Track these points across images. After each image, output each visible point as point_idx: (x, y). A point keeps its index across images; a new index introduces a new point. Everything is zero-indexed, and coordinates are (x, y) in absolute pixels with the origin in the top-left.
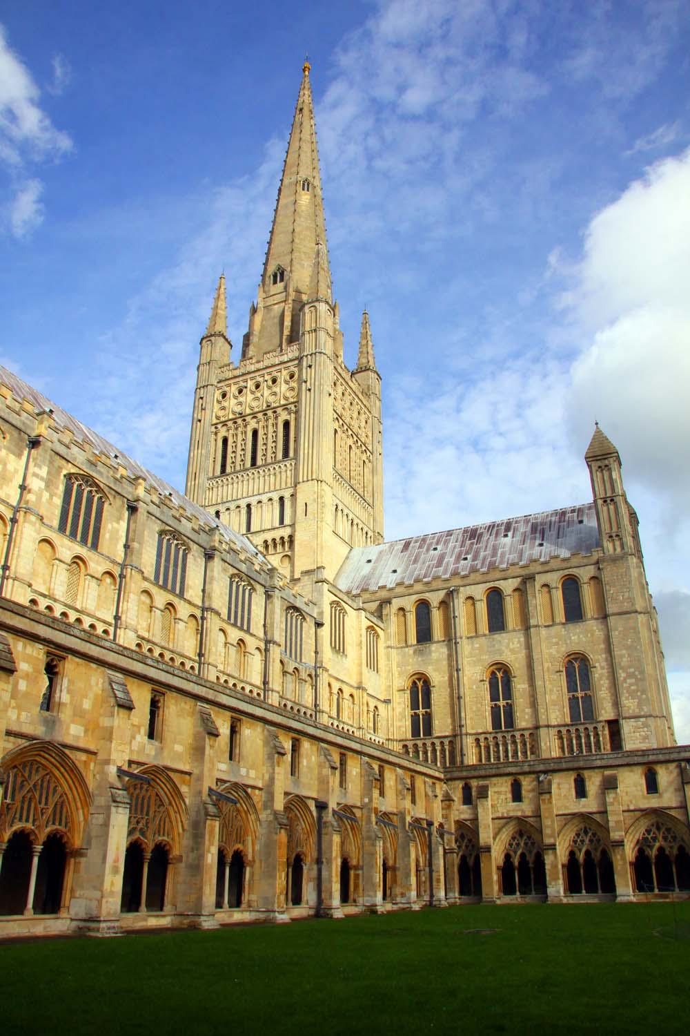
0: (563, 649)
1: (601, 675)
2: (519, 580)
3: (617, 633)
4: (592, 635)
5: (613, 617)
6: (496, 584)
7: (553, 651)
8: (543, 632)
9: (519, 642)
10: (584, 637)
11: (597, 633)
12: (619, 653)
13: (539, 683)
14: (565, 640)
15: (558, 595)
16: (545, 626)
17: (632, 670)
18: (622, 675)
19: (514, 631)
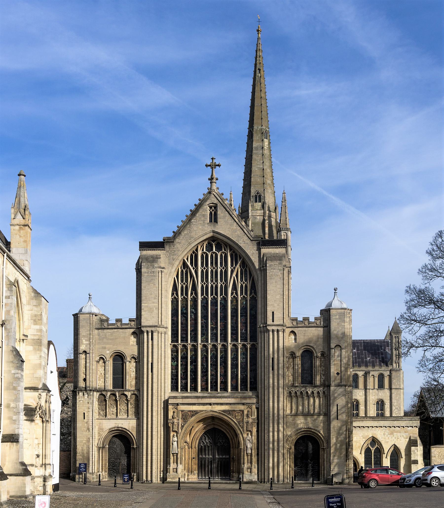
0: (376, 397)
1: (387, 407)
2: (364, 372)
3: (394, 395)
4: (386, 394)
5: (394, 390)
6: (357, 372)
7: (373, 397)
8: (371, 391)
9: (362, 393)
10: (384, 394)
11: (388, 394)
12: (394, 401)
13: (368, 407)
14: (377, 395)
15: (377, 379)
16: (372, 389)
17: (397, 407)
18: (394, 408)
19: (361, 389)
